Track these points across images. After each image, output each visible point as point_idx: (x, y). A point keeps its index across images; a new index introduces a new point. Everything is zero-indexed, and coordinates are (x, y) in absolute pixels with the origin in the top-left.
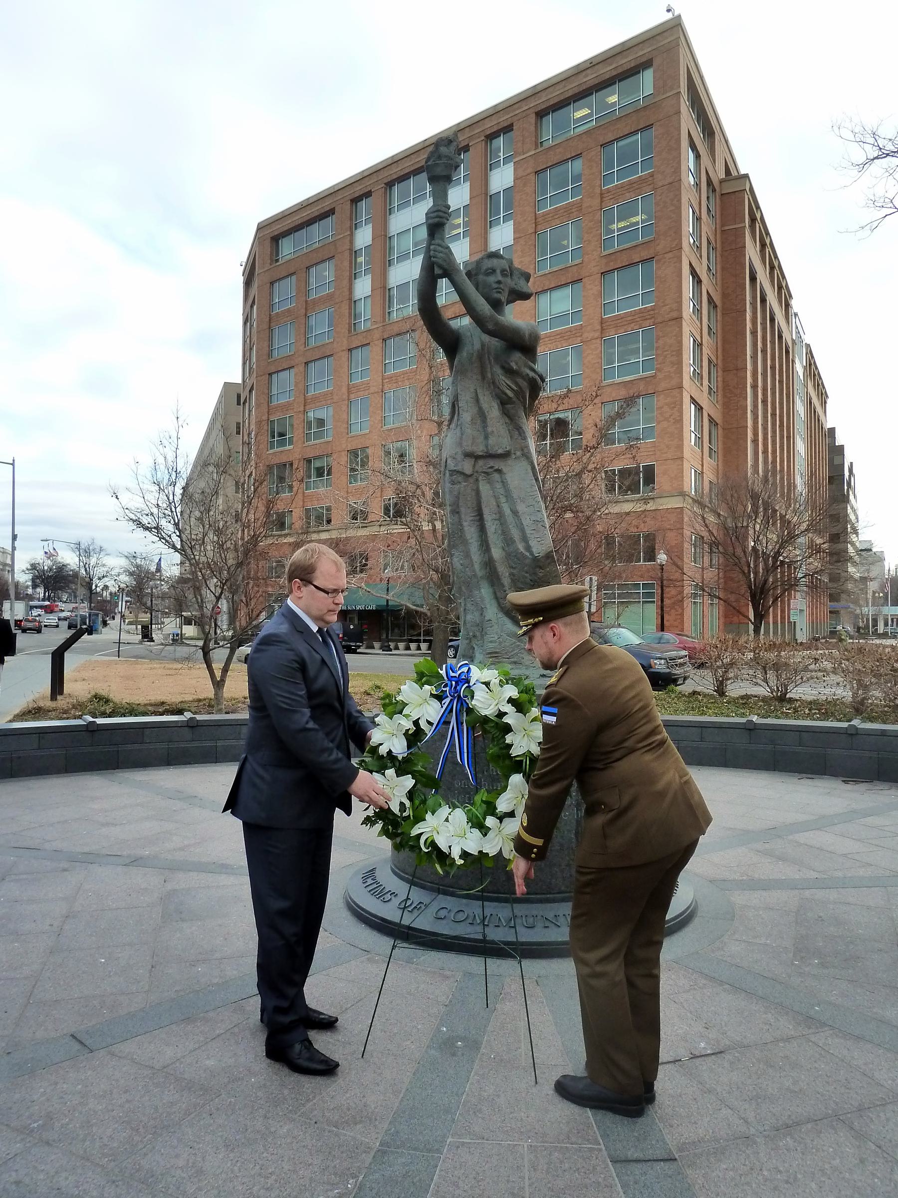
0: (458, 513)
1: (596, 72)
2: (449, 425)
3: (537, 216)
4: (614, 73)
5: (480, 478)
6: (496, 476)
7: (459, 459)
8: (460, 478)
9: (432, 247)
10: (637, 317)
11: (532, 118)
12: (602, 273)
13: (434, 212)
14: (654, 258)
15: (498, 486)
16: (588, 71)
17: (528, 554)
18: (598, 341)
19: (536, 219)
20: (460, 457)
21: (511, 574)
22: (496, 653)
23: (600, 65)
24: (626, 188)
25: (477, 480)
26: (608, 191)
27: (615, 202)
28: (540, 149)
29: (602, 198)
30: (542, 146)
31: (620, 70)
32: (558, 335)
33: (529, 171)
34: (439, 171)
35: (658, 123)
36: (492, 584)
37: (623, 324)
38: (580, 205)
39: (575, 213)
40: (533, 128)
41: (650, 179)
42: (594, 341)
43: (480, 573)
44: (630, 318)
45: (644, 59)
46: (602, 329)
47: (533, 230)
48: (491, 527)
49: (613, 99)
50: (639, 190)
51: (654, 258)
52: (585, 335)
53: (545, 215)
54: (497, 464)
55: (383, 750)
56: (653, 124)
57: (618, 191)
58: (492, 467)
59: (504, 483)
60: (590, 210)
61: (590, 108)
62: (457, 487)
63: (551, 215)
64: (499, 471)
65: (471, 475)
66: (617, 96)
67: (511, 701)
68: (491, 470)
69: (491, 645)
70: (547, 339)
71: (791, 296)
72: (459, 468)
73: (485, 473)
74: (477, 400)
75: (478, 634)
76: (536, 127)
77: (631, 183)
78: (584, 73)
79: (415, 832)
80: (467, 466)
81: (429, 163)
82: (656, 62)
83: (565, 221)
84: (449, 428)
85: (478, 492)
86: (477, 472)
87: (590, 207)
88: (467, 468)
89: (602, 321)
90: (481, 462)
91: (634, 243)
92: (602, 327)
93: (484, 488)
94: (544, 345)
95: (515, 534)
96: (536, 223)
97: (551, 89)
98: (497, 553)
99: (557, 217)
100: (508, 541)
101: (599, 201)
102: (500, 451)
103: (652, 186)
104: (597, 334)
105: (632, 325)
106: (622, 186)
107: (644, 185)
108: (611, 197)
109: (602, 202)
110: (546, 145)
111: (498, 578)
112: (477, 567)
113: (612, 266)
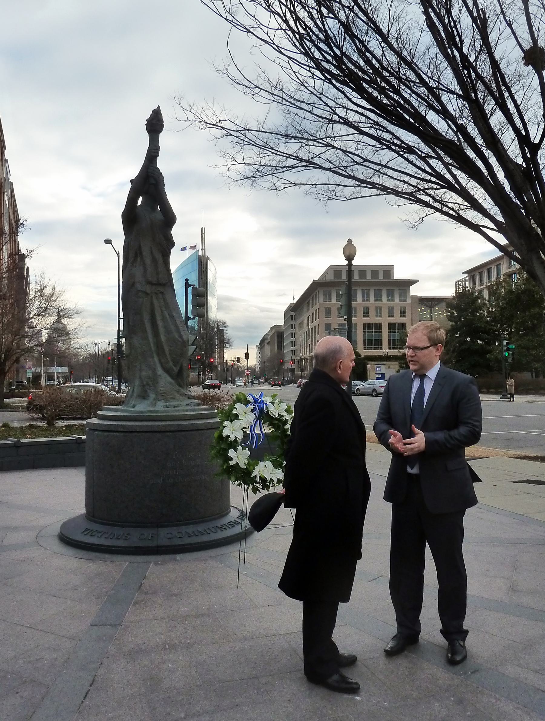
2: (132, 264)
6: (160, 296)
15: (162, 301)
17: (180, 339)
21: (170, 350)
22: (164, 393)
25: (152, 297)
36: (158, 355)
43: (153, 349)
48: (160, 324)
54: (161, 289)
55: (232, 438)
58: (158, 291)
59: (164, 299)
64: (162, 293)
67: (286, 411)
68: (159, 292)
69: (161, 389)
73: (156, 293)
74: (152, 253)
75: (151, 383)
79: (253, 475)
80: (148, 289)
85: (152, 304)
93: (155, 302)
95: (172, 328)
98: (163, 338)
100: (168, 332)
102: (164, 282)
111: (164, 352)
112: (152, 345)
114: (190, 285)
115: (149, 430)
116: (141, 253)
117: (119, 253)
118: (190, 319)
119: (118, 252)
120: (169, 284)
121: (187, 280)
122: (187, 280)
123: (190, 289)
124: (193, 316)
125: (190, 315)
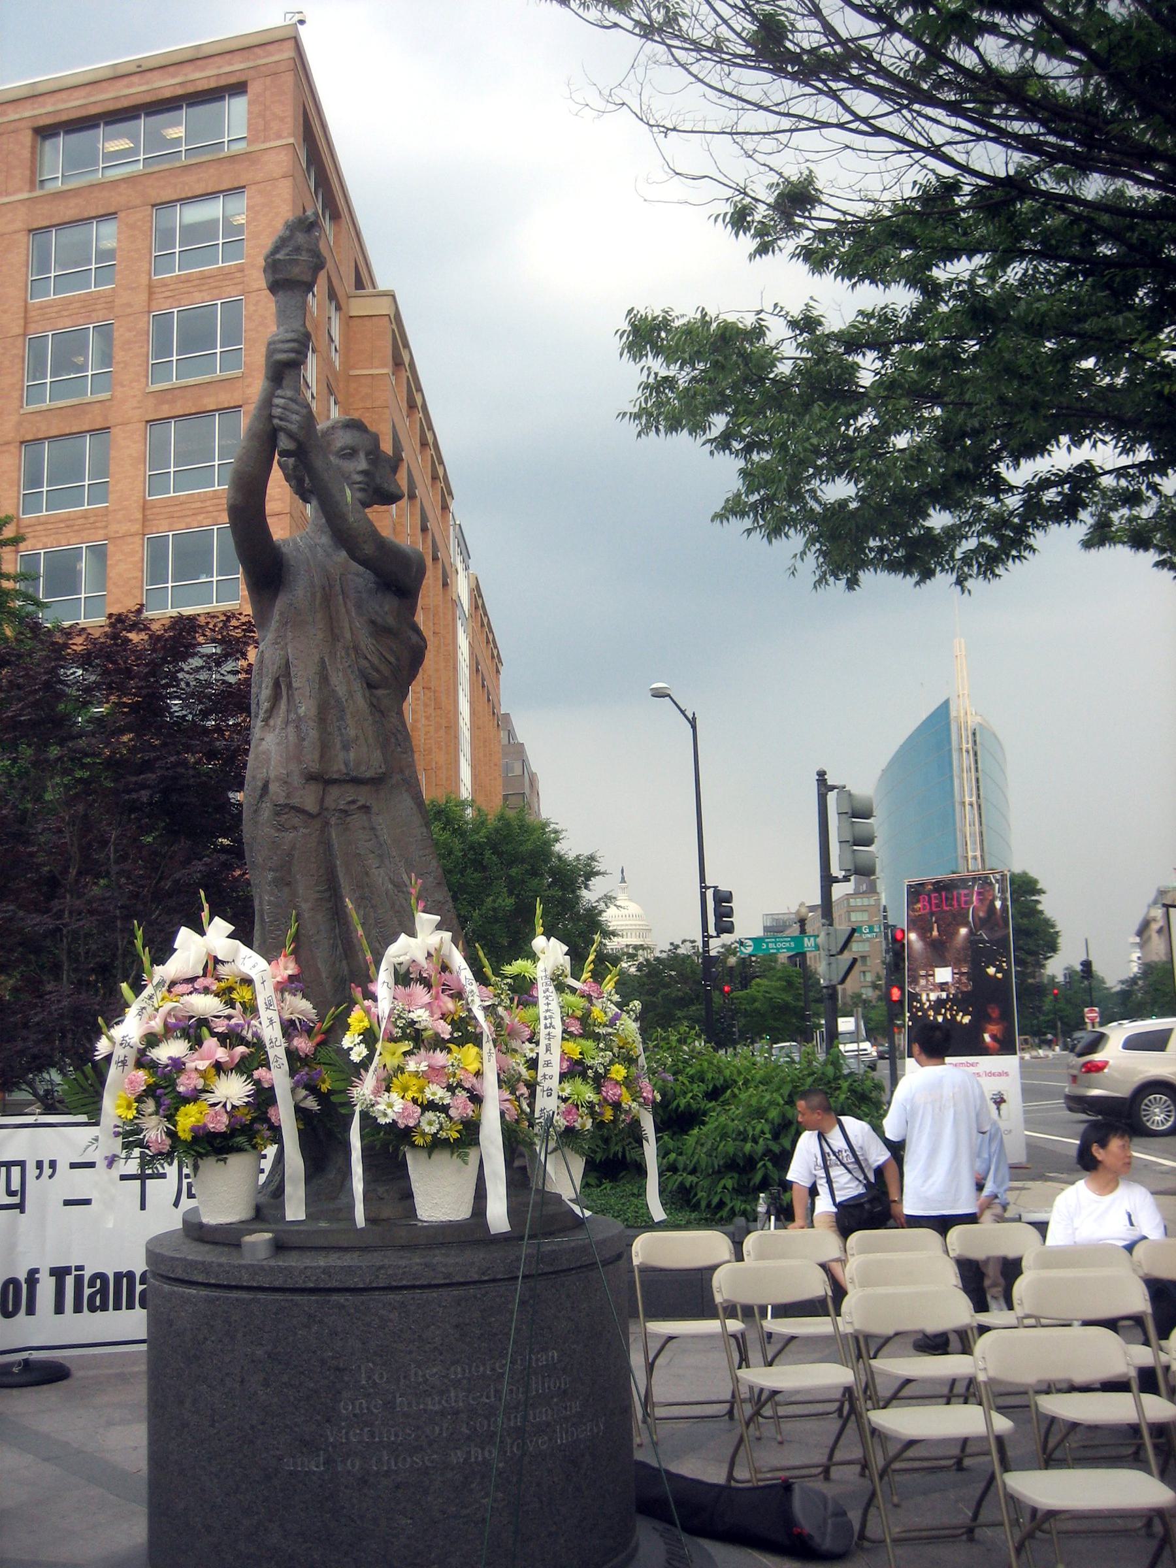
0: (288, 884)
1: (147, 83)
2: (266, 720)
3: (30, 307)
4: (180, 91)
5: (333, 821)
7: (296, 784)
8: (296, 820)
9: (277, 401)
10: (208, 503)
11: (27, 137)
12: (147, 422)
13: (288, 341)
14: (240, 406)
16: (135, 79)
18: (138, 539)
19: (26, 311)
20: (296, 780)
23: (155, 73)
24: (197, 282)
26: (164, 284)
27: (175, 304)
28: (38, 193)
29: (151, 294)
30: (42, 187)
31: (191, 89)
32: (62, 521)
33: (19, 225)
34: (296, 272)
35: (253, 187)
37: (184, 513)
38: (110, 299)
39: (100, 313)
40: (26, 154)
41: (239, 275)
42: (130, 539)
44: (199, 505)
45: (233, 80)
46: (145, 519)
47: (19, 331)
49: (178, 132)
50: (216, 291)
51: (240, 406)
52: (114, 527)
53: (42, 307)
54: (363, 795)
56: (244, 187)
57: (181, 285)
58: (353, 802)
60: (129, 311)
61: (134, 138)
62: (290, 836)
63: (55, 309)
64: (366, 809)
65: (319, 814)
66: (183, 129)
70: (39, 528)
71: (450, 493)
72: (295, 801)
76: (33, 153)
77: (203, 277)
78: (126, 81)
80: (308, 799)
81: (278, 256)
82: (253, 88)
83: (81, 321)
84: (267, 725)
85: (327, 845)
86: (327, 809)
87: (129, 305)
88: (308, 799)
89: (145, 507)
90: (334, 792)
91: (206, 378)
92: (144, 516)
94: (34, 537)
96: (25, 318)
97: (64, 95)
99: (65, 313)
101: (144, 296)
103: (240, 287)
104: (137, 527)
105: (200, 518)
106: (187, 280)
107: (227, 283)
108: (169, 294)
109: (150, 299)
110: (51, 187)
113: (165, 411)
114: (833, 788)
115: (277, 1284)
116: (289, 686)
117: (694, 718)
118: (836, 880)
119: (690, 717)
120: (397, 777)
121: (822, 774)
122: (822, 774)
123: (832, 797)
124: (843, 873)
125: (836, 871)
